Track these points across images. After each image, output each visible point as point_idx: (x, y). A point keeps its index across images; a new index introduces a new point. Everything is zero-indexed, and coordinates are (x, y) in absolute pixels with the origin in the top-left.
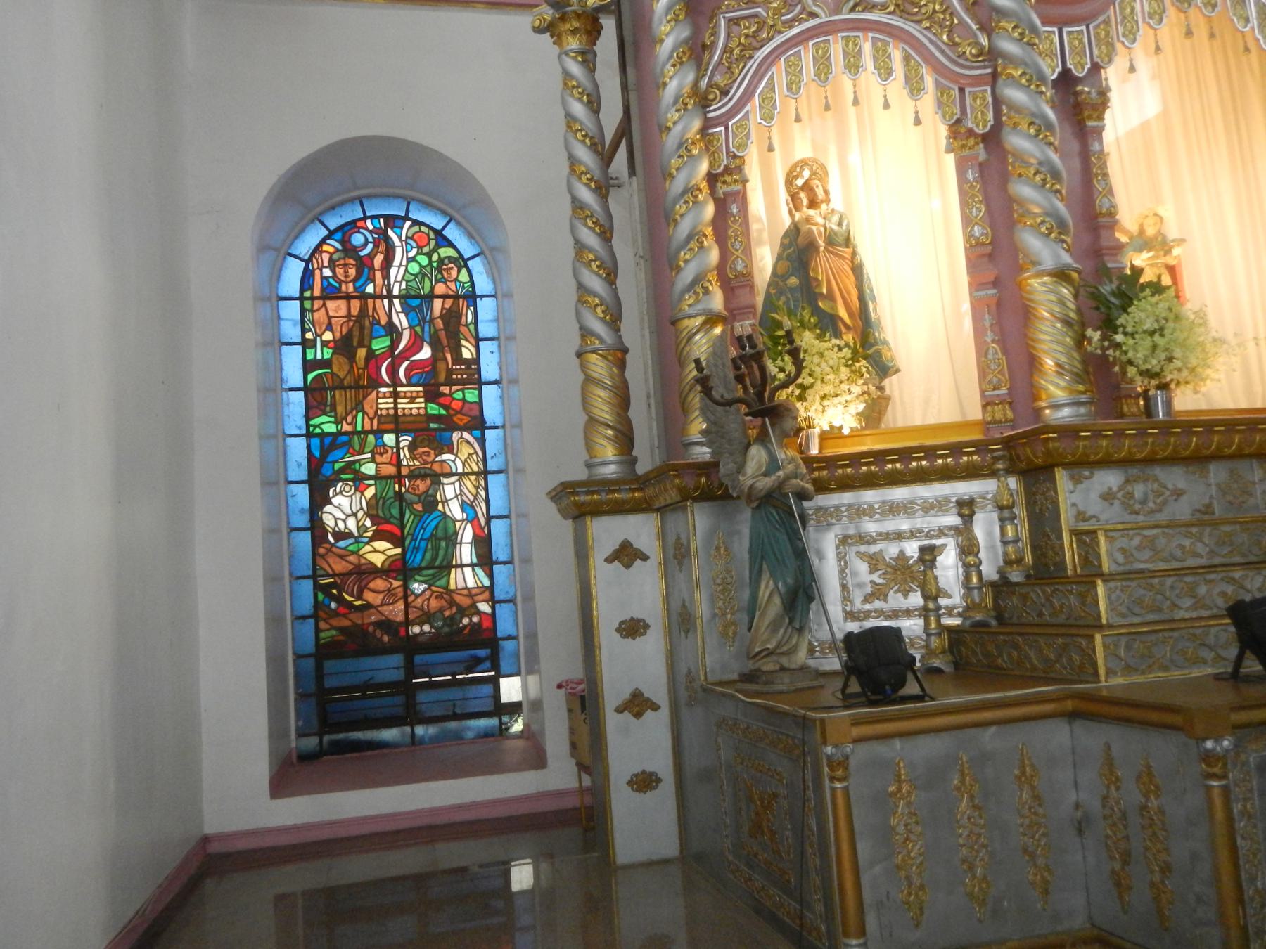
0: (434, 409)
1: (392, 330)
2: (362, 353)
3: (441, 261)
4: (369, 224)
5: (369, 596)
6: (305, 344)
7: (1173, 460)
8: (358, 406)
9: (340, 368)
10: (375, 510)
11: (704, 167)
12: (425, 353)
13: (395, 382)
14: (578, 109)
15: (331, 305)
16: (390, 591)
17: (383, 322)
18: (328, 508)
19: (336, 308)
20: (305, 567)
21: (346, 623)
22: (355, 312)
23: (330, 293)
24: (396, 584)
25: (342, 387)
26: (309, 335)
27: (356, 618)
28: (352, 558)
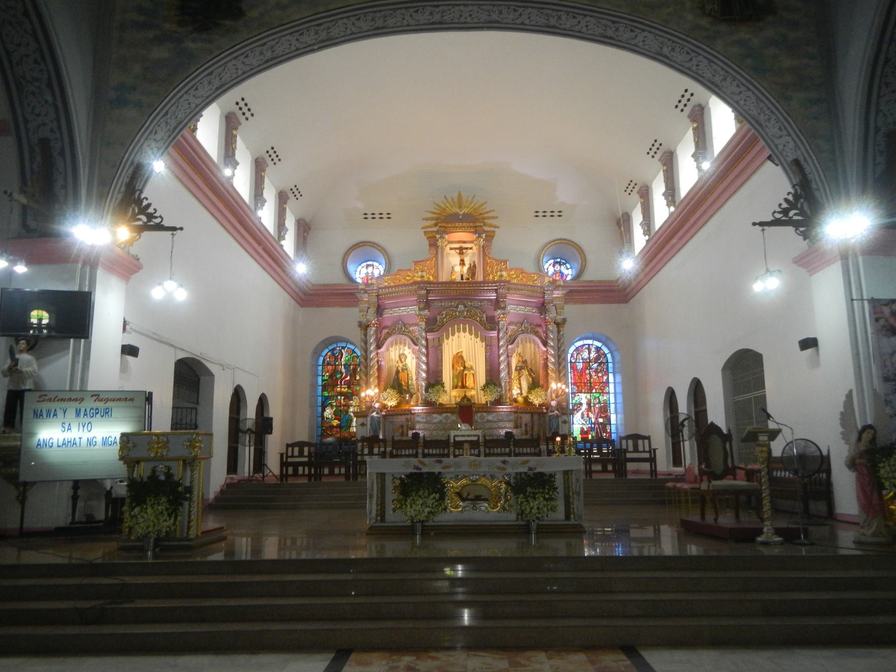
0: (350, 391)
1: (341, 373)
3: (353, 357)
6: (323, 376)
7: (434, 413)
8: (333, 390)
9: (330, 381)
10: (335, 413)
11: (376, 359)
12: (348, 378)
13: (341, 385)
14: (363, 344)
15: (329, 367)
16: (337, 431)
19: (330, 367)
20: (320, 425)
23: (328, 364)
24: (339, 430)
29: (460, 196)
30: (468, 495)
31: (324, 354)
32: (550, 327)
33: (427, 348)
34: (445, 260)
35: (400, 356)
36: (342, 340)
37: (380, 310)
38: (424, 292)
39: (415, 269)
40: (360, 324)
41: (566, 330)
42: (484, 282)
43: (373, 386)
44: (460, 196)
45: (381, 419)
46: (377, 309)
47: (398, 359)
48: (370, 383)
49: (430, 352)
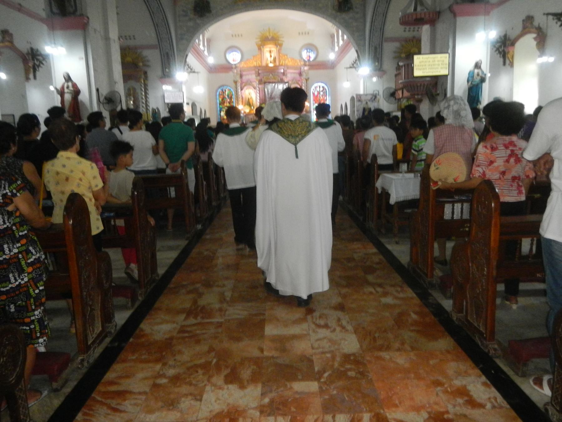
1: (226, 98)
14: (235, 89)
29: (269, 28)
32: (303, 82)
33: (259, 91)
34: (264, 55)
35: (249, 94)
36: (226, 85)
37: (241, 76)
38: (257, 70)
39: (253, 59)
41: (309, 81)
42: (280, 65)
43: (240, 104)
44: (269, 28)
45: (244, 117)
46: (240, 76)
47: (248, 94)
48: (239, 104)
49: (260, 92)
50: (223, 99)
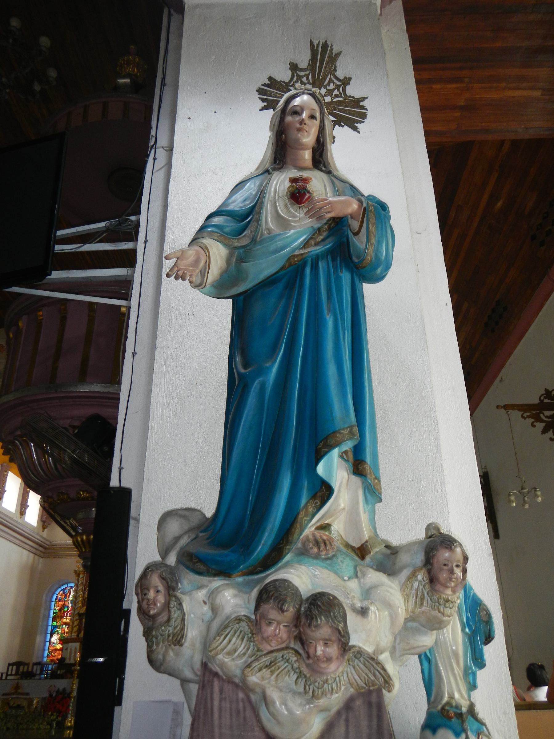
1: (68, 607)
2: (63, 611)
4: (68, 588)
5: (56, 654)
10: (60, 640)
13: (67, 616)
16: (59, 653)
17: (67, 605)
18: (52, 638)
19: (60, 603)
21: (52, 659)
22: (63, 603)
23: (60, 600)
24: (61, 652)
25: (58, 617)
26: (55, 608)
27: (53, 658)
28: (55, 647)
30: (14, 704)
31: (57, 593)
40: (75, 571)
50: (64, 606)
